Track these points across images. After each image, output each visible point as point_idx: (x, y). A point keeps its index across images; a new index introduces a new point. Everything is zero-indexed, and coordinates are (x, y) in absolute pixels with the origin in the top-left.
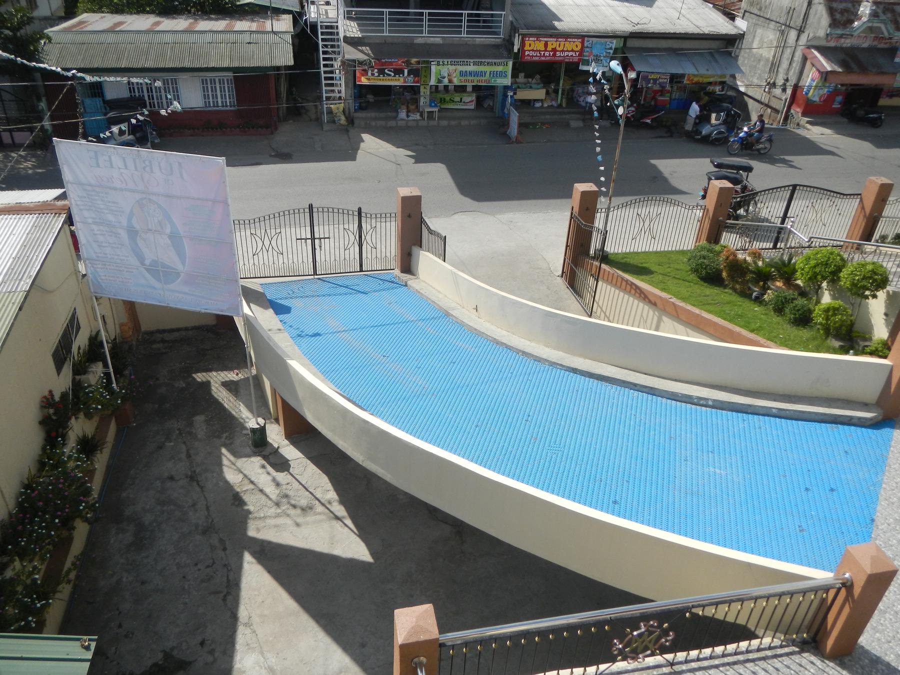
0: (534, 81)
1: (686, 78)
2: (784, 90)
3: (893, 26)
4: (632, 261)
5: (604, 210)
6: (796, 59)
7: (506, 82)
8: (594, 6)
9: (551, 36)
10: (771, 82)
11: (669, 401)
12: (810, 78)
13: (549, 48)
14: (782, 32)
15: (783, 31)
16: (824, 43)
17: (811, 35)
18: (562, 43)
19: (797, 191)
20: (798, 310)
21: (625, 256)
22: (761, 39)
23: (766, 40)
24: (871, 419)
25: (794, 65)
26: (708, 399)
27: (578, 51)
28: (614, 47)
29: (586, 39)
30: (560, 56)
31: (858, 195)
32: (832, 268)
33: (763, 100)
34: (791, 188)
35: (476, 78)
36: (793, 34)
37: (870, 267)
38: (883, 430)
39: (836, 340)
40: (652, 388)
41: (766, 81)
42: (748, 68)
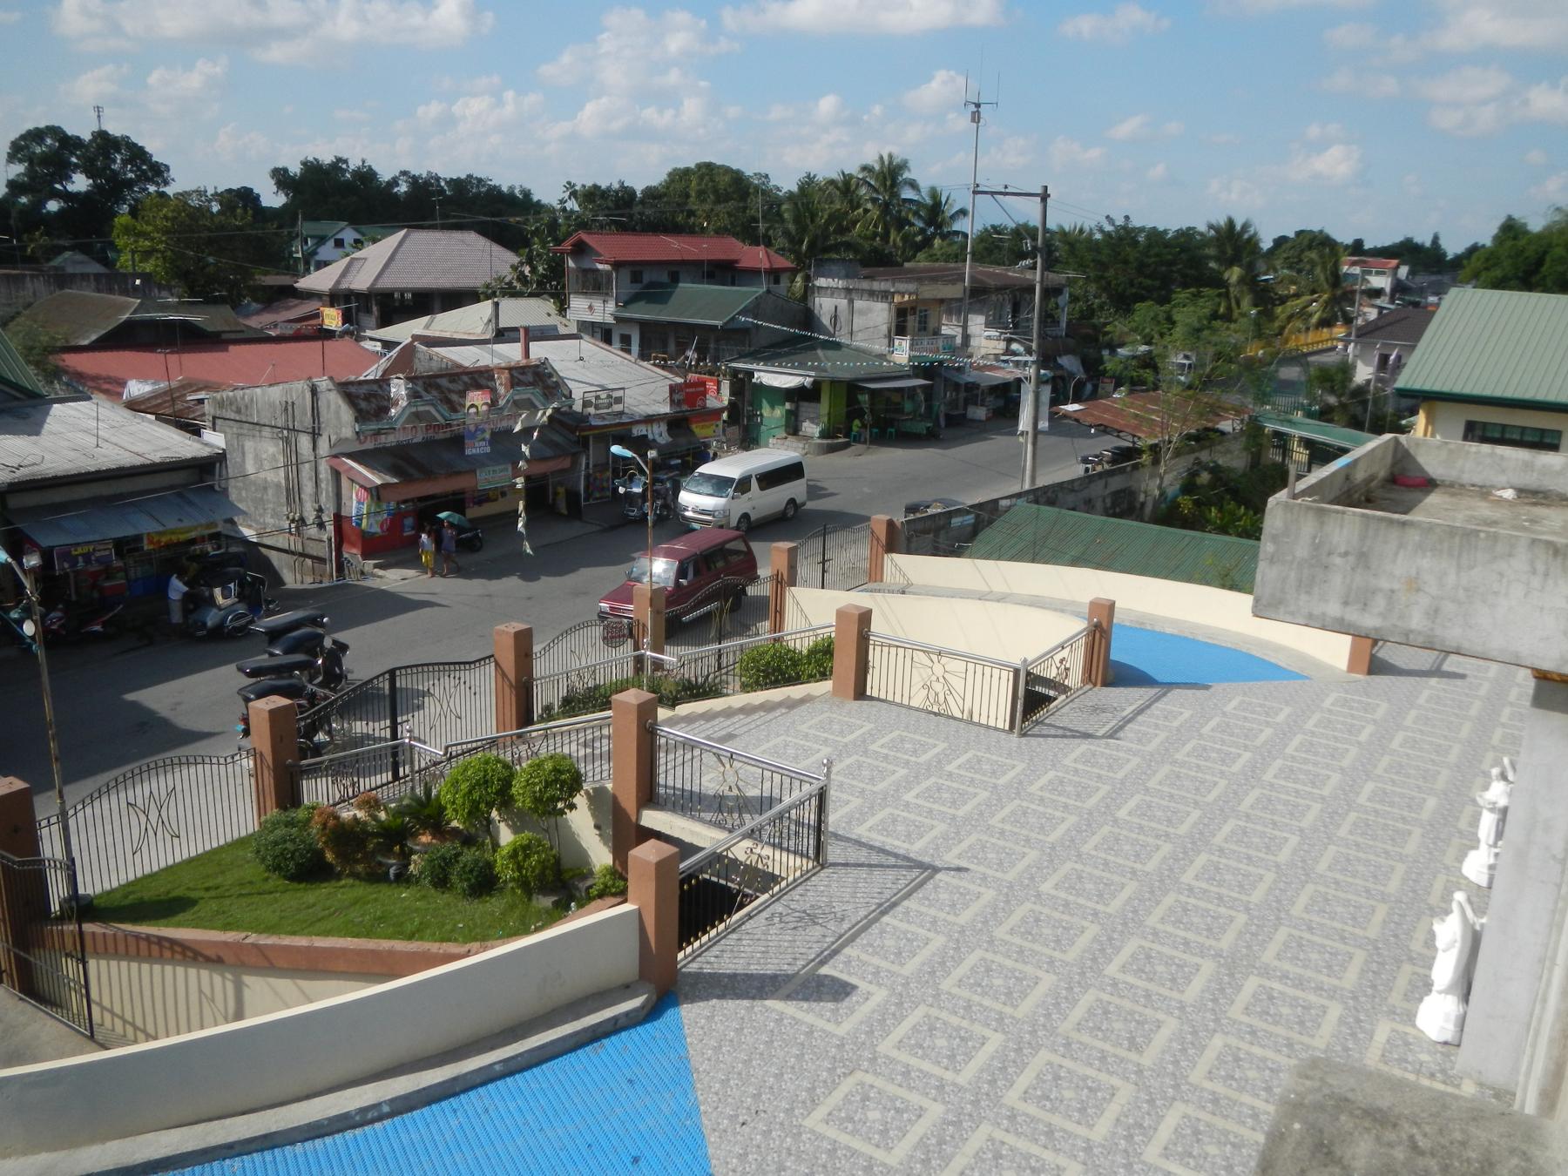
1: (145, 541)
2: (321, 525)
4: (148, 895)
5: (54, 820)
6: (322, 476)
11: (308, 1145)
12: (355, 504)
14: (287, 441)
15: (287, 438)
16: (357, 447)
17: (333, 438)
19: (398, 679)
20: (471, 871)
21: (131, 889)
22: (256, 456)
23: (264, 456)
24: (643, 1007)
25: (323, 485)
26: (380, 1104)
31: (489, 657)
32: (496, 786)
33: (293, 548)
34: (387, 676)
36: (305, 442)
37: (549, 766)
38: (665, 1015)
39: (545, 895)
40: (265, 1137)
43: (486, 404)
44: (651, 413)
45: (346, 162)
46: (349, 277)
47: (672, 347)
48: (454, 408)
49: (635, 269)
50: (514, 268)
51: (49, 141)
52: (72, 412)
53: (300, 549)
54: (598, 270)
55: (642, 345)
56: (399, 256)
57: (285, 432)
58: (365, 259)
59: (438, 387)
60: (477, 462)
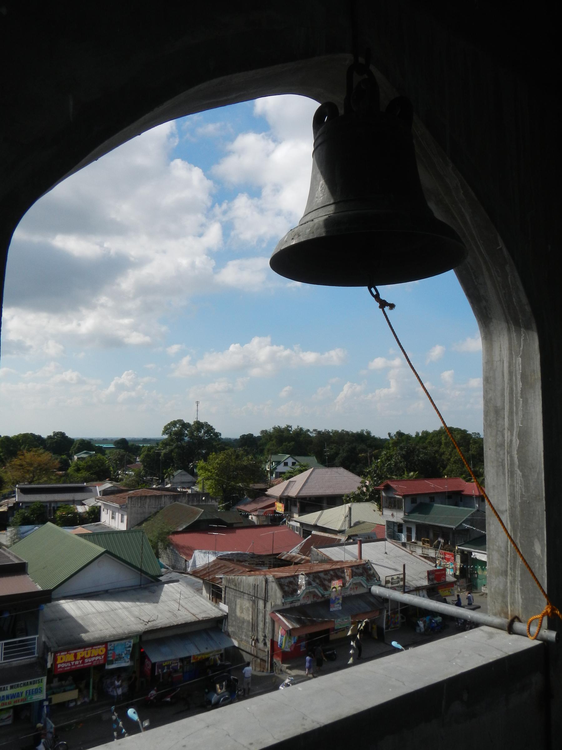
0: (67, 682)
1: (192, 658)
2: (265, 644)
3: (322, 588)
6: (267, 620)
7: (42, 697)
8: (113, 610)
9: (79, 648)
10: (255, 639)
12: (280, 637)
13: (79, 657)
14: (254, 602)
15: (254, 600)
16: (281, 608)
17: (273, 604)
18: (89, 652)
23: (244, 607)
25: (267, 625)
27: (103, 655)
28: (132, 645)
29: (109, 644)
30: (88, 662)
35: (13, 700)
36: (261, 603)
41: (251, 638)
42: (236, 628)
43: (340, 586)
44: (419, 585)
45: (291, 427)
46: (288, 490)
47: (431, 535)
48: (326, 588)
49: (413, 498)
50: (359, 488)
51: (178, 425)
52: (171, 589)
53: (255, 654)
54: (396, 498)
55: (417, 534)
56: (309, 480)
57: (254, 598)
58: (295, 481)
59: (319, 578)
60: (335, 615)
